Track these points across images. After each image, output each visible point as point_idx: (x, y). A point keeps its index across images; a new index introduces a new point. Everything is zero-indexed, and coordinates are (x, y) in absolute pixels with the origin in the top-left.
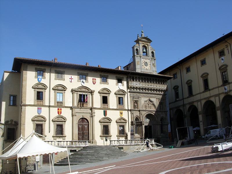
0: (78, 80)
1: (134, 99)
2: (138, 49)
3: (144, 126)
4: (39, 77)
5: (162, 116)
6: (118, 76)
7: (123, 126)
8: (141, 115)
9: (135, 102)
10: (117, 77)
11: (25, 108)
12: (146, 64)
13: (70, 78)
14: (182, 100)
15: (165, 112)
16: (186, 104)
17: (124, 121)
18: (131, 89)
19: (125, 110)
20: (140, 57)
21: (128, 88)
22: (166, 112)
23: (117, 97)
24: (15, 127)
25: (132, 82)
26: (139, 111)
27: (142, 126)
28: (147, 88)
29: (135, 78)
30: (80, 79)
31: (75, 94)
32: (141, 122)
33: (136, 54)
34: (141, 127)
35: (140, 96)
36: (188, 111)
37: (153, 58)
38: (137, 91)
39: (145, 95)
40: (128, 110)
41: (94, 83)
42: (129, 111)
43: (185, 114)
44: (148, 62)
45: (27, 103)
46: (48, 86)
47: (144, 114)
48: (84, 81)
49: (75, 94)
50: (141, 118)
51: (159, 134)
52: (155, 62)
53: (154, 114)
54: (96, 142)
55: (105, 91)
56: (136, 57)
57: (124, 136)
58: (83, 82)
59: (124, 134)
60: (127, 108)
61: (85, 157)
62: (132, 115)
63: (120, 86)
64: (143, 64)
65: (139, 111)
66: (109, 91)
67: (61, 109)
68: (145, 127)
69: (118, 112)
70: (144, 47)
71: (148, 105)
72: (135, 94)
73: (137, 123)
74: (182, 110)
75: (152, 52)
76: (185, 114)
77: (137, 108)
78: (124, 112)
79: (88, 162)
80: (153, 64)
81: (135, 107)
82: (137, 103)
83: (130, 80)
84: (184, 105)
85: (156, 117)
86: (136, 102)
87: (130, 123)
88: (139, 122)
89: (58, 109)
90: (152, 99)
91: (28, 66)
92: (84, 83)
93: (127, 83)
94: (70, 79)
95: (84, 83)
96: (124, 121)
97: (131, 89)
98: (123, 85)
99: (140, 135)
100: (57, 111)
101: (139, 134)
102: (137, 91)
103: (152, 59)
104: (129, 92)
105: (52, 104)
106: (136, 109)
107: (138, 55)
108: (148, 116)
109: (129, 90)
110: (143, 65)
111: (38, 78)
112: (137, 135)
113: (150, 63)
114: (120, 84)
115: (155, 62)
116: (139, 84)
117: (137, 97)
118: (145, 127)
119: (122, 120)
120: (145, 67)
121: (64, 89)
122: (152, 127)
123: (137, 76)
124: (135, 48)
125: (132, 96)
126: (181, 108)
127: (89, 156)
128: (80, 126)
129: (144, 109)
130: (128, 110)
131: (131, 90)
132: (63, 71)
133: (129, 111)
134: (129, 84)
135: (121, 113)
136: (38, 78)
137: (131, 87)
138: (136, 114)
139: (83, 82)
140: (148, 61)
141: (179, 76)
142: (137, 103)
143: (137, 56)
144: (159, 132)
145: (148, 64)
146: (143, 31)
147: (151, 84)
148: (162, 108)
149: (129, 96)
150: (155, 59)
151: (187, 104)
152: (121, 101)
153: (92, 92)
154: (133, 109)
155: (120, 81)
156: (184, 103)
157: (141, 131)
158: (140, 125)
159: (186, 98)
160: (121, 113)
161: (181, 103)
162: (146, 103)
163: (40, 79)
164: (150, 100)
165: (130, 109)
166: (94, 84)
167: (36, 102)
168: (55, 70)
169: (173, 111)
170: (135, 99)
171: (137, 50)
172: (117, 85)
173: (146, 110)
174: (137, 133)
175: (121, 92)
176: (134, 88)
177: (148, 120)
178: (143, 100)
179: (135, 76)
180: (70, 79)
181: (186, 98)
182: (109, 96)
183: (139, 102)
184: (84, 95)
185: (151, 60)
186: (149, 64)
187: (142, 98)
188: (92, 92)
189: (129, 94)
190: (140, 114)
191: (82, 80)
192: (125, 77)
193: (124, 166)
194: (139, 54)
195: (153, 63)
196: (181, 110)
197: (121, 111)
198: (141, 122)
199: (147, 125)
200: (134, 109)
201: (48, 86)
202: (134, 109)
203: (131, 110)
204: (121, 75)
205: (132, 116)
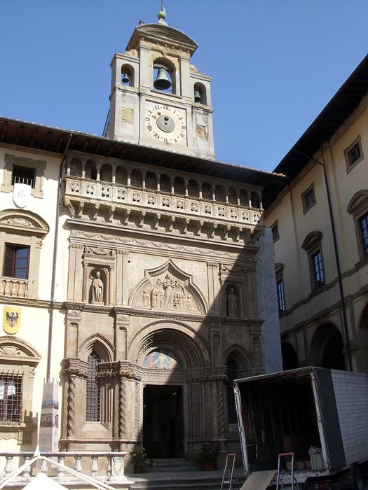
1: (88, 259)
2: (135, 66)
5: (232, 342)
6: (18, 154)
7: (17, 381)
8: (120, 333)
9: (93, 274)
14: (337, 285)
15: (249, 323)
16: (352, 297)
17: (23, 356)
18: (77, 213)
19: (35, 303)
20: (140, 95)
21: (62, 207)
22: (252, 327)
25: (84, 184)
26: (113, 313)
27: (120, 383)
28: (159, 214)
29: (99, 168)
32: (117, 366)
33: (119, 83)
34: (117, 387)
35: (125, 249)
36: (361, 326)
37: (198, 105)
39: (149, 244)
40: (51, 306)
42: (56, 312)
43: (348, 340)
44: (176, 119)
50: (121, 348)
51: (216, 429)
52: (206, 122)
53: (192, 335)
56: (119, 93)
57: (15, 430)
59: (16, 418)
60: (44, 295)
62: (72, 329)
64: (153, 123)
65: (113, 313)
68: (150, 391)
70: (161, 63)
71: (165, 288)
72: (97, 236)
73: (99, 368)
74: (339, 327)
75: (199, 88)
76: (351, 338)
78: (25, 312)
80: (199, 129)
82: (103, 278)
83: (76, 174)
84: (344, 303)
85: (201, 346)
86: (100, 272)
87: (56, 369)
88: (108, 367)
90: (183, 266)
93: (60, 186)
96: (23, 356)
97: (77, 213)
99: (110, 425)
103: (193, 107)
104: (69, 226)
106: (99, 304)
108: (163, 341)
109: (64, 218)
110: (150, 128)
112: (95, 429)
113: (184, 121)
114: (21, 187)
115: (206, 122)
116: (117, 194)
117: (107, 251)
118: (150, 391)
119: (12, 350)
122: (185, 391)
123: (114, 162)
124: (120, 63)
125: (82, 243)
126: (335, 319)
129: (143, 306)
130: (51, 306)
131: (77, 216)
133: (56, 312)
134: (68, 191)
135: (11, 318)
137: (76, 205)
138: (102, 325)
140: (175, 114)
141: (320, 193)
142: (103, 278)
143: (124, 91)
144: (215, 414)
145: (173, 125)
146: (163, 13)
147: (181, 199)
148: (232, 306)
149: (63, 244)
150: (207, 112)
151: (358, 295)
152: (19, 264)
154: (78, 300)
156: (345, 295)
157: (117, 408)
158: (113, 377)
159: (350, 273)
160: (11, 318)
161: (331, 298)
162: (153, 280)
165: (61, 297)
169: (305, 333)
171: (127, 70)
173: (153, 310)
174: (94, 414)
175: (23, 222)
176: (89, 209)
177: (166, 362)
178: (134, 269)
179: (100, 161)
181: (350, 273)
183: (113, 272)
185: (189, 110)
186: (179, 125)
187: (135, 258)
189: (65, 234)
190: (115, 327)
192: (53, 163)
194: (136, 84)
195: (201, 122)
196: (332, 326)
197: (13, 309)
198: (117, 366)
199: (161, 380)
200: (86, 302)
202: (86, 302)
203: (65, 307)
204: (36, 153)
205: (72, 337)
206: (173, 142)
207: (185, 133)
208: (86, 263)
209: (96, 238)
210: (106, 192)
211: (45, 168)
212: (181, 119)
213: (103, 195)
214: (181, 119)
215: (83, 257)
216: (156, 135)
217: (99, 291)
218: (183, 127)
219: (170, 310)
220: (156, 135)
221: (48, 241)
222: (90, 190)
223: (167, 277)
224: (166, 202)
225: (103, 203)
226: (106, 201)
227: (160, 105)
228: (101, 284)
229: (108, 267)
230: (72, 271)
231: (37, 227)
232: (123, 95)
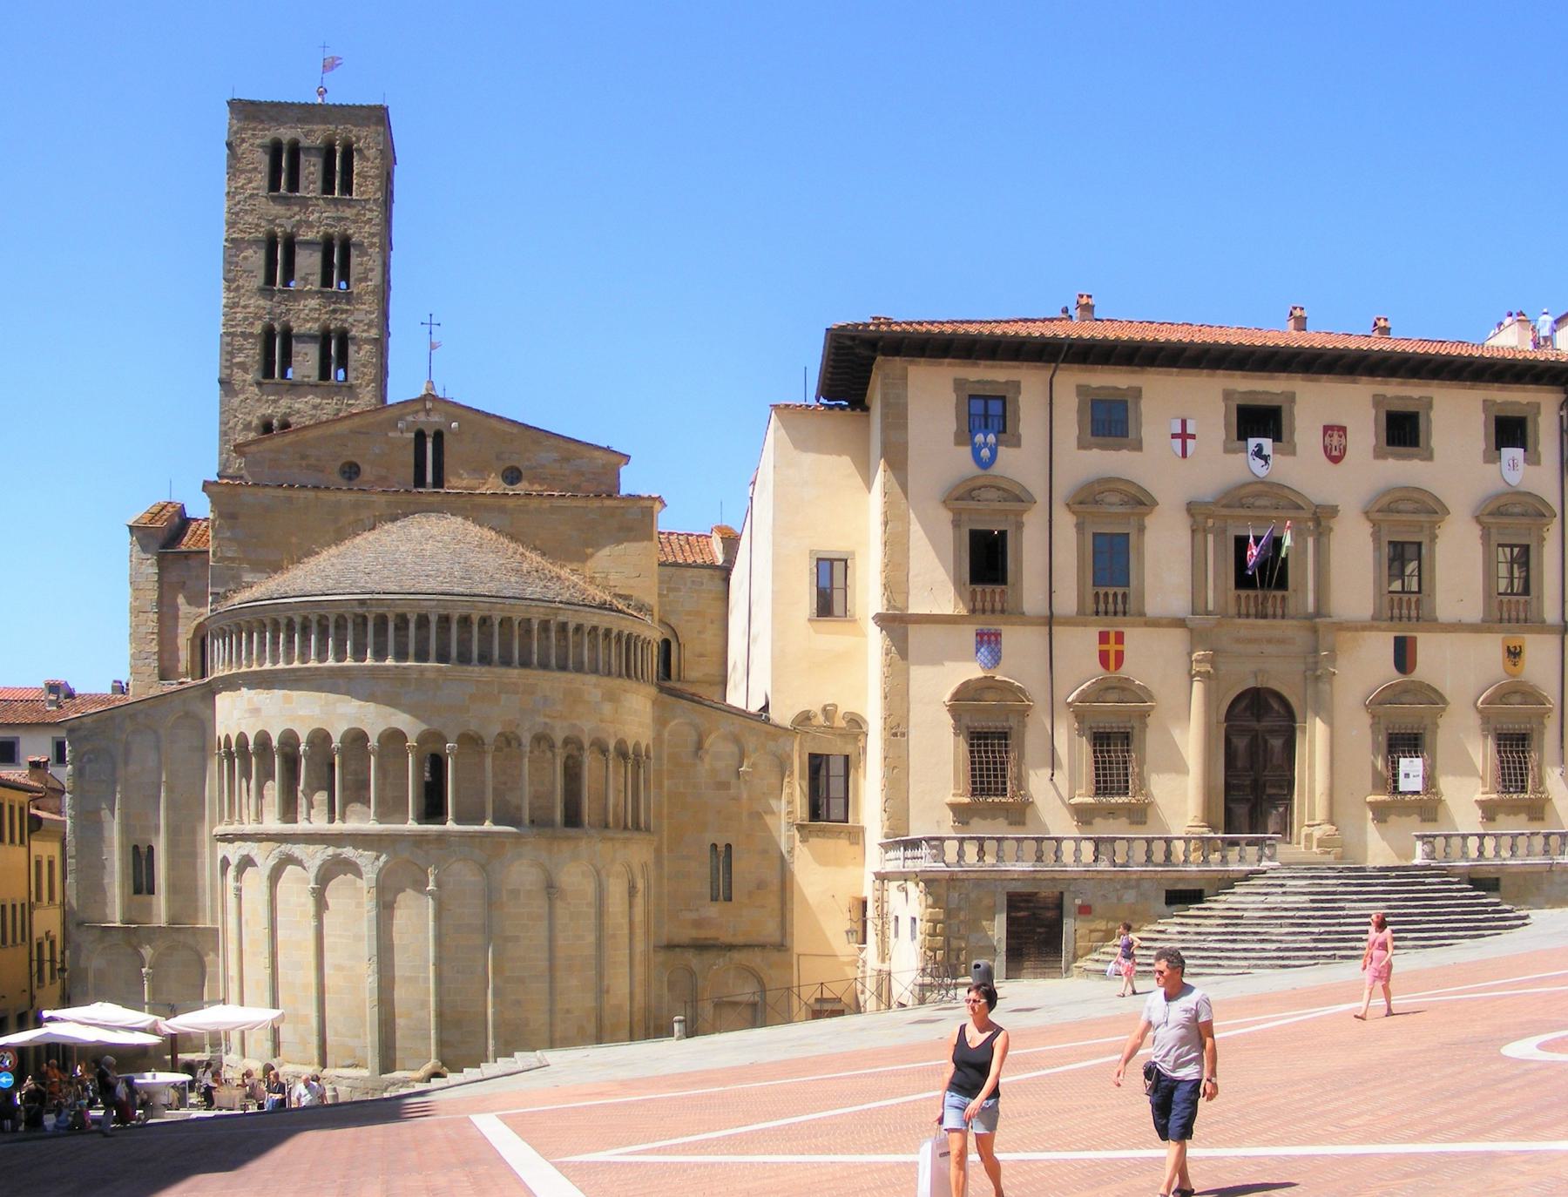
0: (1225, 442)
4: (979, 438)
10: (1494, 403)
13: (1179, 431)
24: (849, 750)
30: (1239, 438)
31: (1210, 538)
41: (1335, 453)
46: (1041, 496)
48: (1267, 444)
49: (1210, 538)
58: (1259, 453)
61: (1256, 933)
63: (1514, 466)
66: (1431, 509)
67: (1120, 638)
69: (1491, 647)
79: (1267, 962)
89: (1104, 637)
91: (910, 368)
92: (1265, 458)
94: (1174, 436)
95: (1265, 458)
98: (1533, 459)
100: (1094, 647)
105: (1067, 601)
111: (973, 444)
121: (1140, 502)
127: (1281, 926)
128: (1241, 743)
136: (973, 444)
139: (1259, 453)
153: (1320, 519)
155: (1510, 431)
163: (985, 453)
166: (1336, 460)
168: (1078, 387)
172: (1492, 456)
180: (1174, 436)
188: (1320, 519)
191: (1253, 442)
193: (1457, 993)
201: (1038, 490)
211: (1539, 413)
231: (1533, 510)
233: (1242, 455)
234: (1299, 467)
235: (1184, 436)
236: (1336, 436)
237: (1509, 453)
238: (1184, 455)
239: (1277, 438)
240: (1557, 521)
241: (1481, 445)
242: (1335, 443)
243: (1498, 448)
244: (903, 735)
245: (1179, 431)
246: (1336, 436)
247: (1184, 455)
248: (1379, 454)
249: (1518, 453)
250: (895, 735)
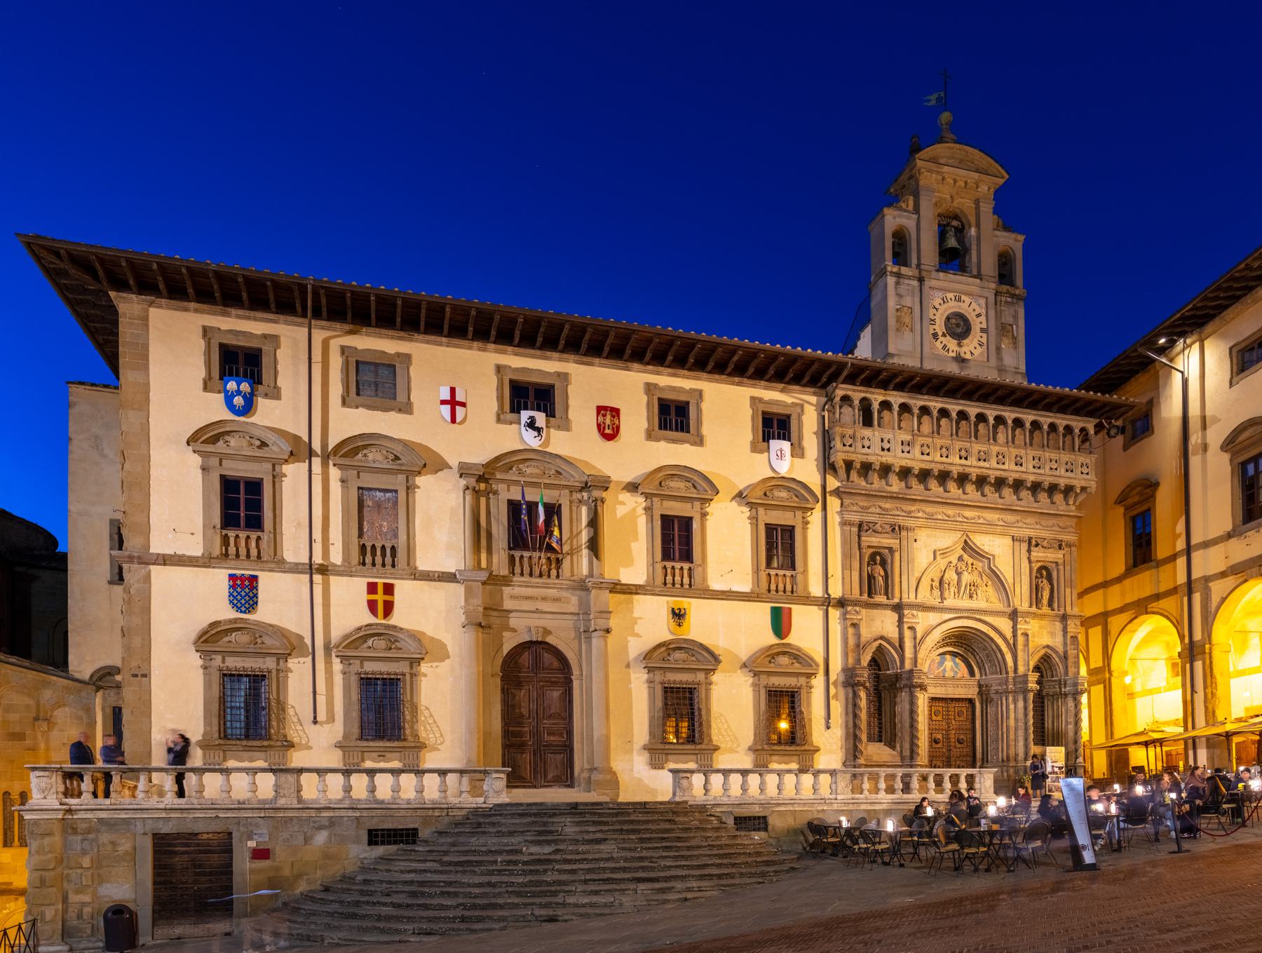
3: (922, 700)
11: (147, 579)
12: (959, 327)
21: (828, 466)
23: (754, 520)
28: (955, 471)
30: (512, 411)
35: (910, 523)
38: (889, 489)
41: (607, 431)
45: (157, 547)
47: (931, 627)
52: (1015, 317)
54: (614, 782)
55: (678, 486)
71: (959, 574)
77: (886, 594)
81: (870, 585)
86: (880, 559)
90: (984, 542)
92: (539, 430)
95: (539, 430)
98: (798, 451)
100: (364, 597)
101: (891, 744)
102: (889, 489)
104: (837, 493)
107: (904, 270)
109: (833, 483)
113: (983, 318)
120: (952, 344)
132: (398, 355)
136: (226, 392)
137: (849, 465)
142: (883, 563)
149: (834, 520)
164: (968, 547)
166: (609, 438)
167: (218, 541)
170: (870, 540)
176: (866, 468)
177: (951, 666)
182: (704, 515)
183: (897, 555)
184: (532, 506)
187: (922, 535)
189: (834, 503)
202: (865, 597)
206: (968, 356)
207: (984, 340)
208: (864, 544)
209: (872, 510)
210: (886, 446)
212: (979, 315)
213: (883, 449)
214: (979, 315)
215: (859, 537)
216: (945, 347)
217: (880, 581)
218: (982, 330)
219: (965, 603)
220: (945, 347)
221: (815, 517)
222: (867, 443)
223: (960, 559)
224: (963, 453)
225: (884, 460)
226: (887, 458)
227: (950, 295)
228: (882, 573)
229: (891, 550)
230: (847, 556)
232: (897, 283)
233: (514, 426)
234: (575, 441)
235: (453, 403)
236: (608, 417)
237: (776, 445)
238: (453, 420)
239: (550, 414)
240: (819, 506)
241: (749, 437)
242: (608, 421)
243: (767, 438)
244: (145, 676)
245: (448, 398)
246: (608, 417)
247: (453, 420)
248: (650, 436)
249: (786, 445)
250: (136, 676)
